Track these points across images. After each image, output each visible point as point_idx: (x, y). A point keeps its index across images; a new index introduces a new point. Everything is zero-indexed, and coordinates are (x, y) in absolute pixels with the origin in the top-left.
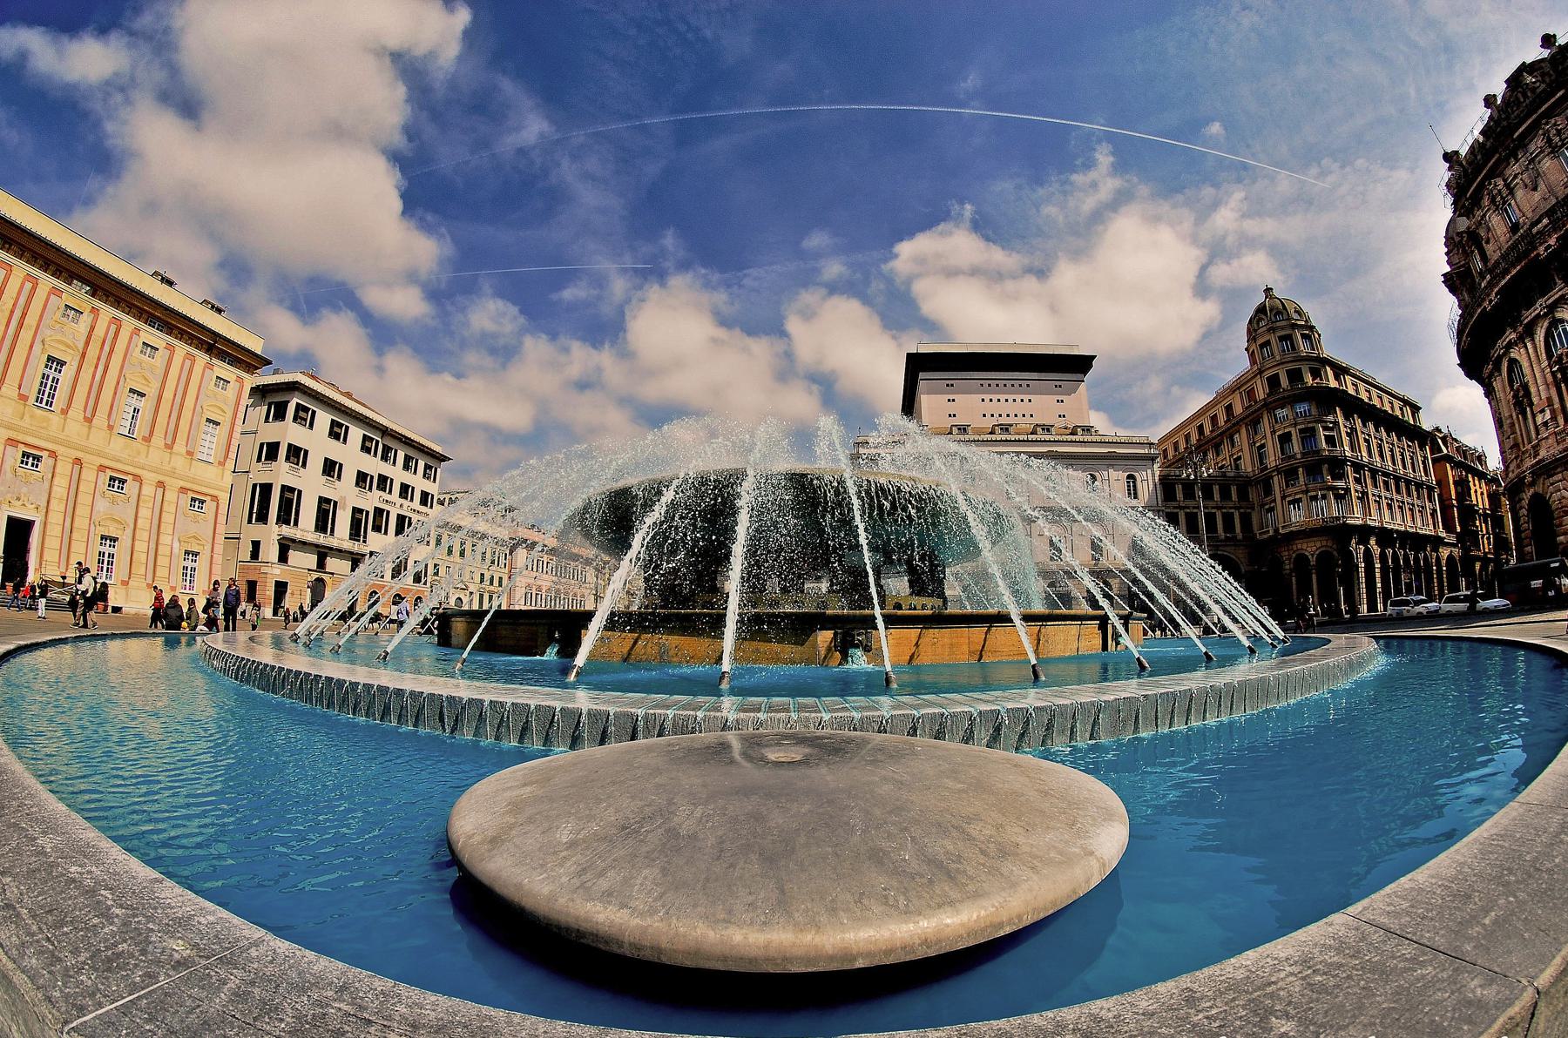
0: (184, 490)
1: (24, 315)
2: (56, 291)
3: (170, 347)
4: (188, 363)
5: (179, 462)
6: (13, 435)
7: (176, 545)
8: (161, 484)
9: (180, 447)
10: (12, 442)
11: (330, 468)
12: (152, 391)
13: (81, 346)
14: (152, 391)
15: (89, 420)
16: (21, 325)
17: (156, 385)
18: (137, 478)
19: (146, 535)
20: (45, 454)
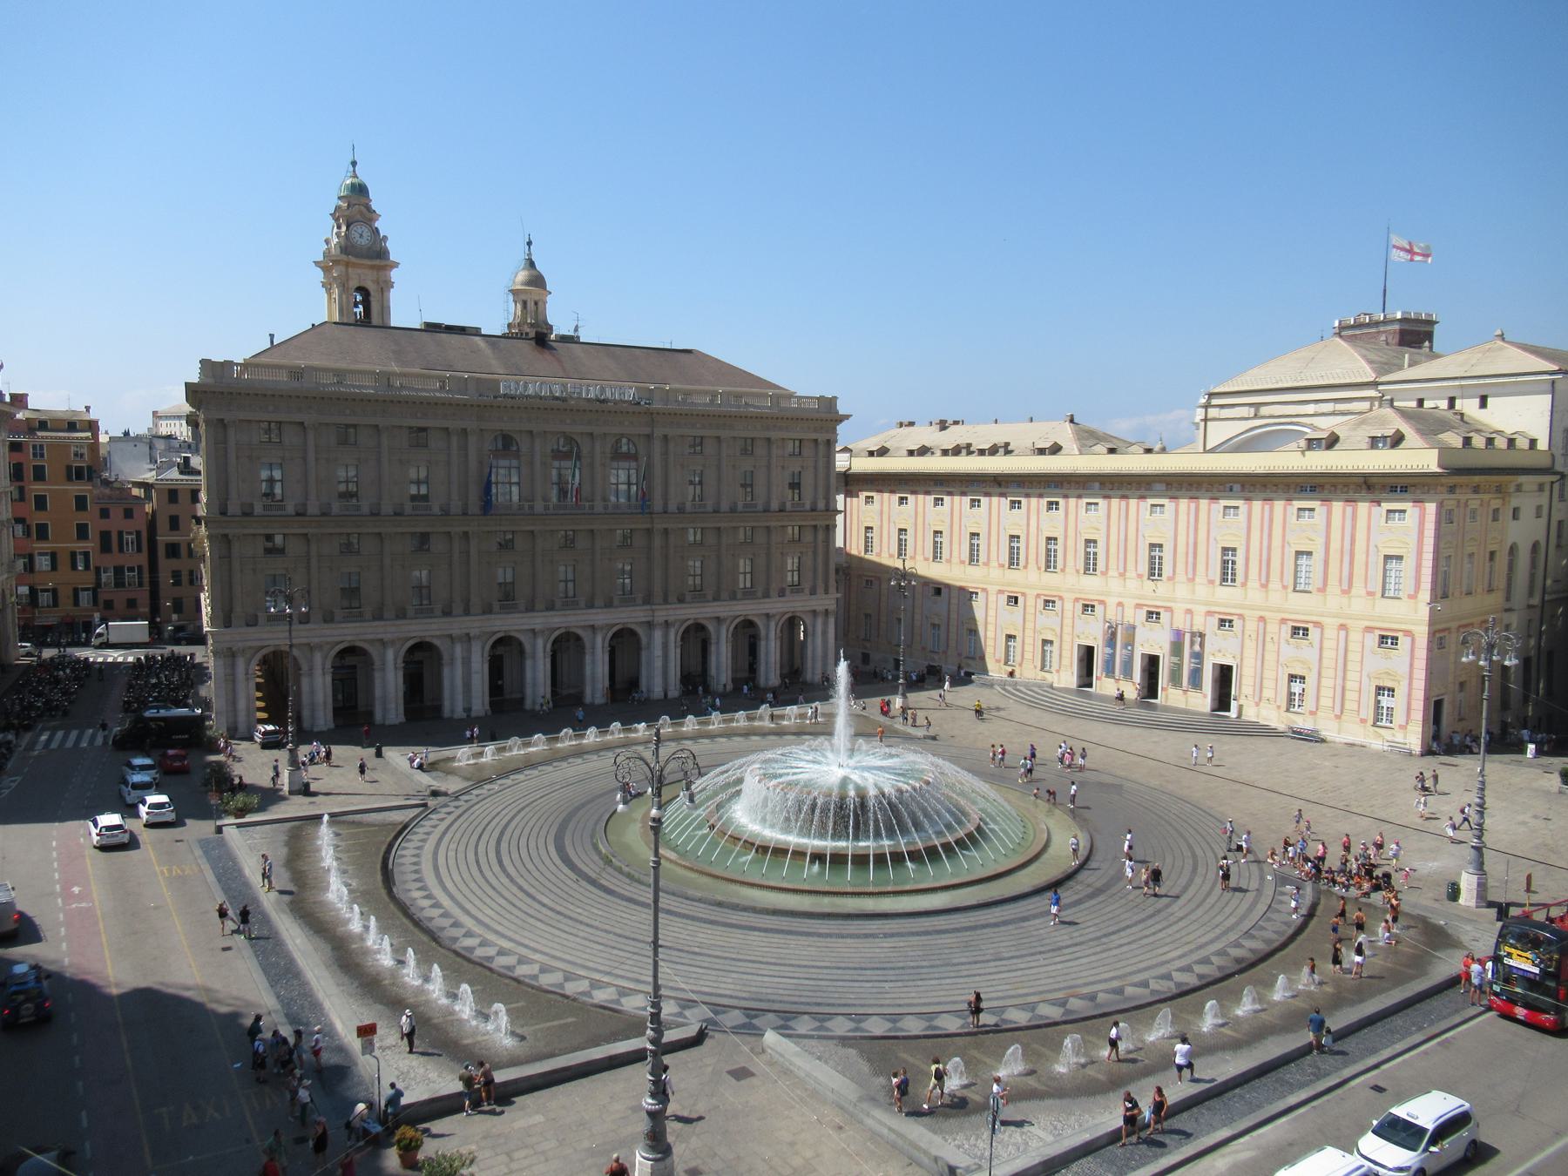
0: (1369, 629)
7: (1365, 679)
10: (1210, 613)
12: (1318, 548)
14: (1318, 548)
15: (1265, 586)
17: (1321, 541)
18: (1317, 624)
19: (1331, 673)
20: (1234, 618)
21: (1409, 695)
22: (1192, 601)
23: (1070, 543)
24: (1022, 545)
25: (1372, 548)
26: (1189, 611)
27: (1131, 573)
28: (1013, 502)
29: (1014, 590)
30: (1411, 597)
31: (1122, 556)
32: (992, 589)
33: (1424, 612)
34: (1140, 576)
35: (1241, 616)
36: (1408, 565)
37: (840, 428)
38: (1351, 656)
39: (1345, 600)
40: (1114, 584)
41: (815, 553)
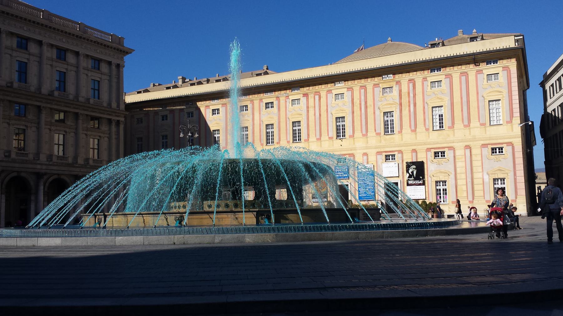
1: (366, 103)
2: (376, 85)
3: (449, 76)
4: (463, 78)
5: (476, 131)
6: (379, 150)
7: (486, 177)
8: (468, 147)
9: (475, 123)
10: (379, 153)
12: (446, 102)
13: (397, 101)
15: (414, 131)
16: (366, 107)
18: (450, 148)
19: (463, 176)
20: (396, 153)
21: (515, 179)
22: (367, 148)
24: (250, 132)
25: (481, 98)
31: (318, 128)
34: (331, 138)
35: (400, 152)
37: (127, 58)
38: (475, 164)
39: (467, 131)
41: (110, 138)
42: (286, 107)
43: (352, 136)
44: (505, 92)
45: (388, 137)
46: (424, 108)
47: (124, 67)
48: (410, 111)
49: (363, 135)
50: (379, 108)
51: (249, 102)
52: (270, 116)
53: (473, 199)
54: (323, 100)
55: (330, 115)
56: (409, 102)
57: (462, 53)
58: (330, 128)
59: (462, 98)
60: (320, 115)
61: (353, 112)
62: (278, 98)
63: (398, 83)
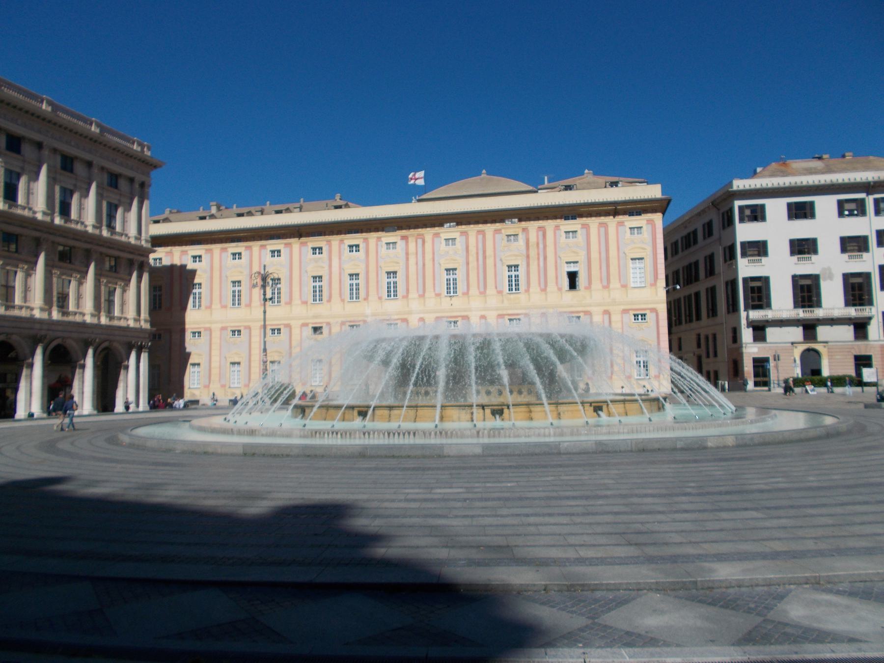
0: (625, 311)
2: (497, 231)
3: (586, 226)
5: (617, 293)
6: (501, 312)
8: (607, 312)
9: (615, 284)
11: (803, 247)
12: (582, 257)
13: (525, 252)
15: (544, 290)
16: (485, 258)
18: (587, 313)
23: (372, 275)
24: (325, 283)
25: (621, 255)
26: (483, 317)
27: (430, 293)
28: (314, 249)
29: (317, 322)
30: (652, 285)
32: (296, 324)
33: (662, 294)
34: (438, 295)
36: (649, 261)
37: (154, 174)
40: (415, 304)
42: (377, 252)
43: (466, 294)
44: (649, 249)
45: (512, 296)
46: (556, 262)
47: (150, 186)
48: (539, 265)
49: (481, 293)
50: (501, 260)
51: (325, 243)
52: (354, 262)
53: (612, 374)
54: (428, 245)
55: (437, 265)
56: (538, 254)
57: (601, 200)
58: (436, 282)
59: (600, 253)
60: (424, 265)
61: (468, 264)
62: (366, 240)
63: (525, 230)
